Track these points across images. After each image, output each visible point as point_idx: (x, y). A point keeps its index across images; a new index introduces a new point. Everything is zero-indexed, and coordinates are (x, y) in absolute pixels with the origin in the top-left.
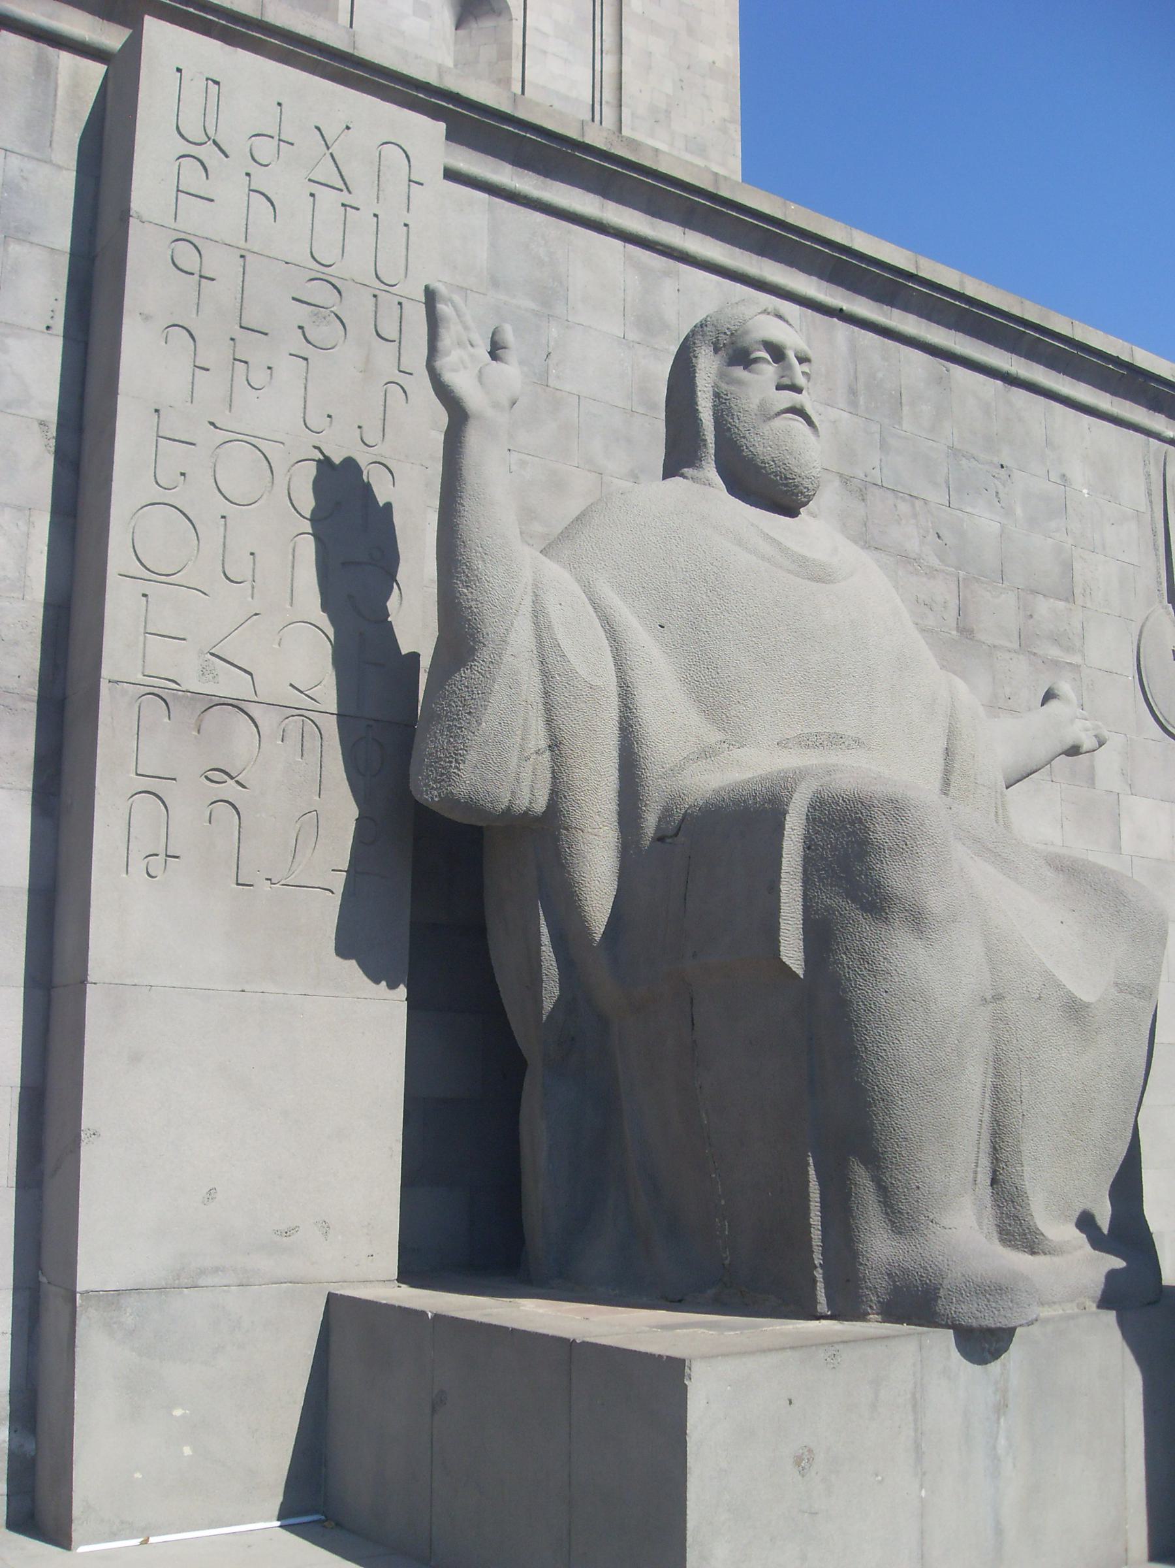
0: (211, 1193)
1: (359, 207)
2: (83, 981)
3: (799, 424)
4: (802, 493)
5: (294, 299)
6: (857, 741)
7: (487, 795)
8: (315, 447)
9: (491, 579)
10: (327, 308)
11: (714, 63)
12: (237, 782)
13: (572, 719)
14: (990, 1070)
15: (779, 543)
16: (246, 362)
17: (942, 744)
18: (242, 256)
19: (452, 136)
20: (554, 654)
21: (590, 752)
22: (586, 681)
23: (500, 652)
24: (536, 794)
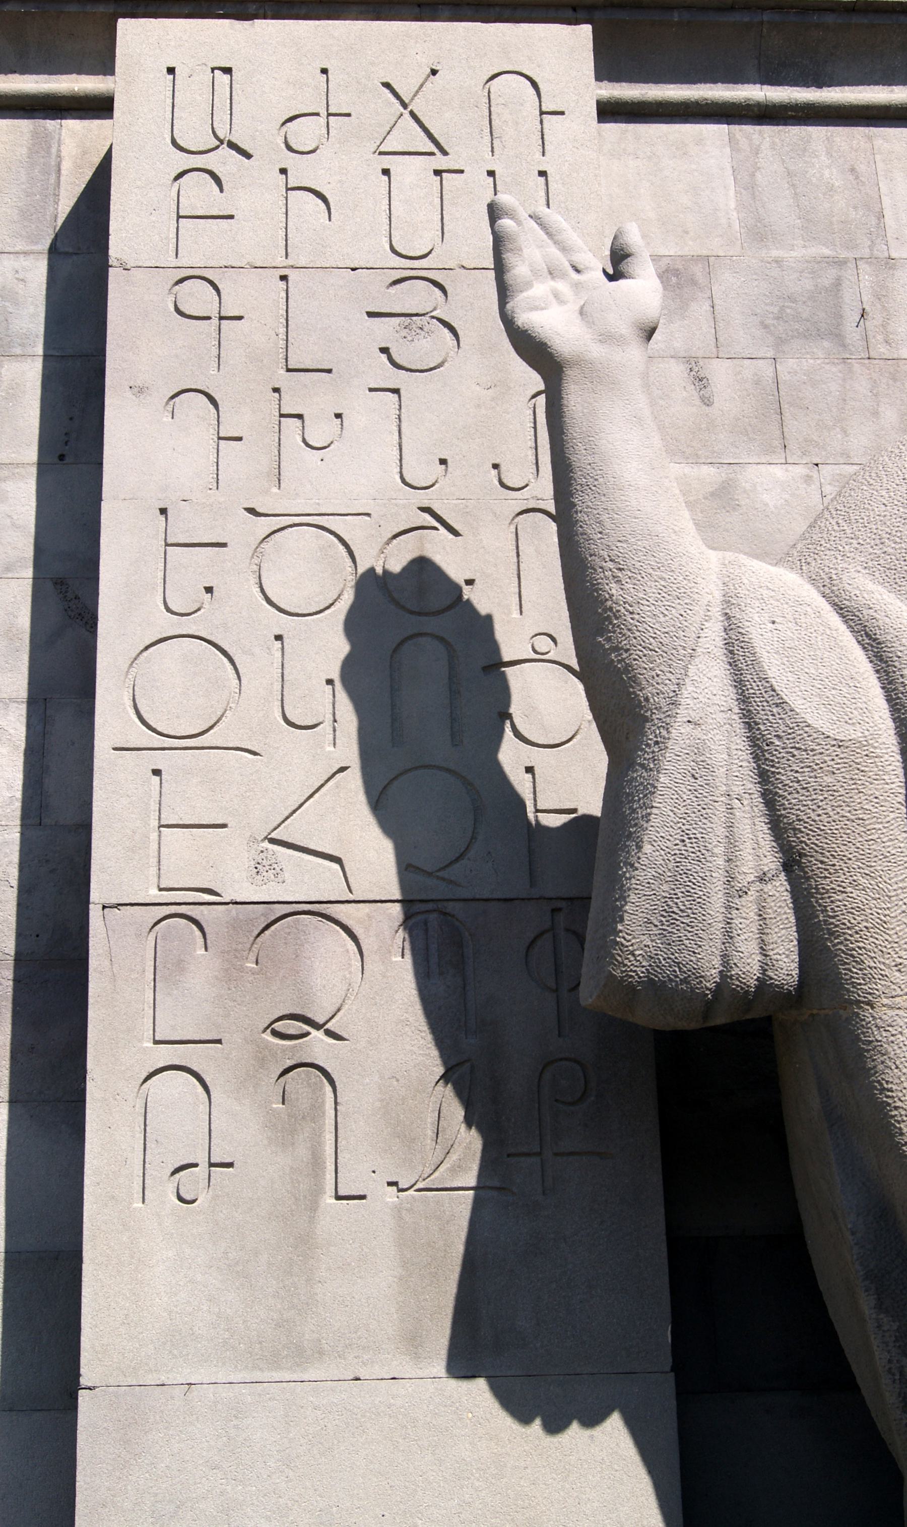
1: (462, 168)
5: (371, 314)
7: (677, 969)
9: (636, 606)
10: (423, 315)
12: (330, 1034)
13: (814, 807)
16: (300, 417)
18: (284, 278)
20: (765, 704)
21: (858, 860)
22: (828, 737)
23: (668, 722)
24: (771, 953)
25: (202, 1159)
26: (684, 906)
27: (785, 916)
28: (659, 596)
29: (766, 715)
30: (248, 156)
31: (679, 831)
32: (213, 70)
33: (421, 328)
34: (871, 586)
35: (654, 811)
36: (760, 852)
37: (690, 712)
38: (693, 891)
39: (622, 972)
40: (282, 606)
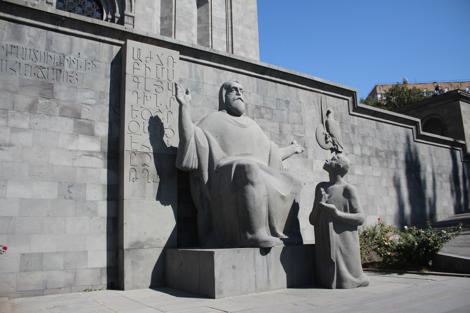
0: (145, 233)
2: (123, 199)
3: (240, 101)
4: (241, 113)
5: (154, 85)
6: (251, 154)
11: (251, 9)
12: (147, 166)
14: (267, 207)
15: (236, 122)
16: (146, 96)
17: (269, 154)
18: (145, 78)
25: (135, 178)
30: (142, 62)
34: (208, 132)
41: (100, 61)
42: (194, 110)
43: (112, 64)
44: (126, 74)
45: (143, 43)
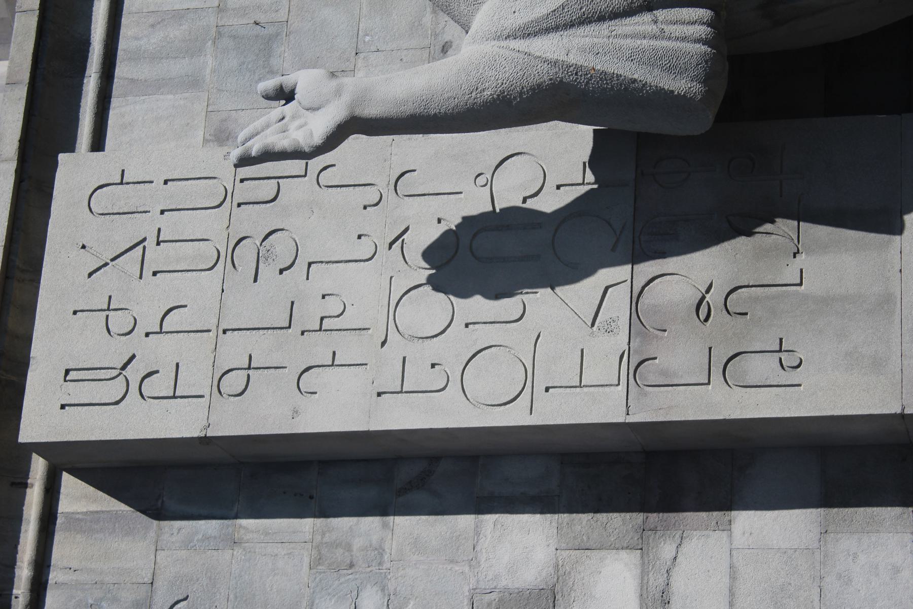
5: (255, 280)
7: (700, 66)
8: (390, 248)
9: (499, 81)
10: (259, 250)
12: (708, 291)
16: (322, 319)
18: (225, 332)
19: (70, 146)
20: (561, 16)
23: (566, 66)
24: (695, 19)
26: (667, 61)
27: (676, 12)
28: (494, 70)
29: (568, 15)
30: (133, 357)
31: (626, 62)
32: (65, 381)
33: (268, 251)
35: (616, 72)
36: (641, 22)
37: (562, 54)
38: (659, 56)
39: (699, 94)
40: (446, 324)
41: (148, 580)
42: (378, 51)
43: (158, 513)
44: (210, 434)
45: (33, 354)
